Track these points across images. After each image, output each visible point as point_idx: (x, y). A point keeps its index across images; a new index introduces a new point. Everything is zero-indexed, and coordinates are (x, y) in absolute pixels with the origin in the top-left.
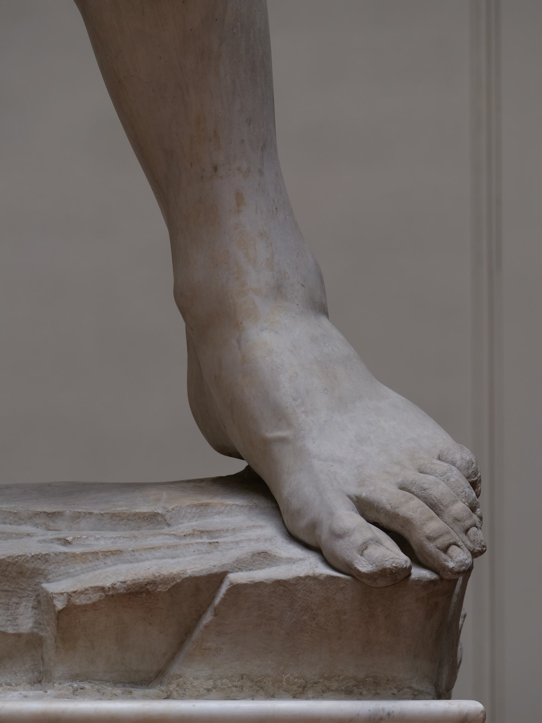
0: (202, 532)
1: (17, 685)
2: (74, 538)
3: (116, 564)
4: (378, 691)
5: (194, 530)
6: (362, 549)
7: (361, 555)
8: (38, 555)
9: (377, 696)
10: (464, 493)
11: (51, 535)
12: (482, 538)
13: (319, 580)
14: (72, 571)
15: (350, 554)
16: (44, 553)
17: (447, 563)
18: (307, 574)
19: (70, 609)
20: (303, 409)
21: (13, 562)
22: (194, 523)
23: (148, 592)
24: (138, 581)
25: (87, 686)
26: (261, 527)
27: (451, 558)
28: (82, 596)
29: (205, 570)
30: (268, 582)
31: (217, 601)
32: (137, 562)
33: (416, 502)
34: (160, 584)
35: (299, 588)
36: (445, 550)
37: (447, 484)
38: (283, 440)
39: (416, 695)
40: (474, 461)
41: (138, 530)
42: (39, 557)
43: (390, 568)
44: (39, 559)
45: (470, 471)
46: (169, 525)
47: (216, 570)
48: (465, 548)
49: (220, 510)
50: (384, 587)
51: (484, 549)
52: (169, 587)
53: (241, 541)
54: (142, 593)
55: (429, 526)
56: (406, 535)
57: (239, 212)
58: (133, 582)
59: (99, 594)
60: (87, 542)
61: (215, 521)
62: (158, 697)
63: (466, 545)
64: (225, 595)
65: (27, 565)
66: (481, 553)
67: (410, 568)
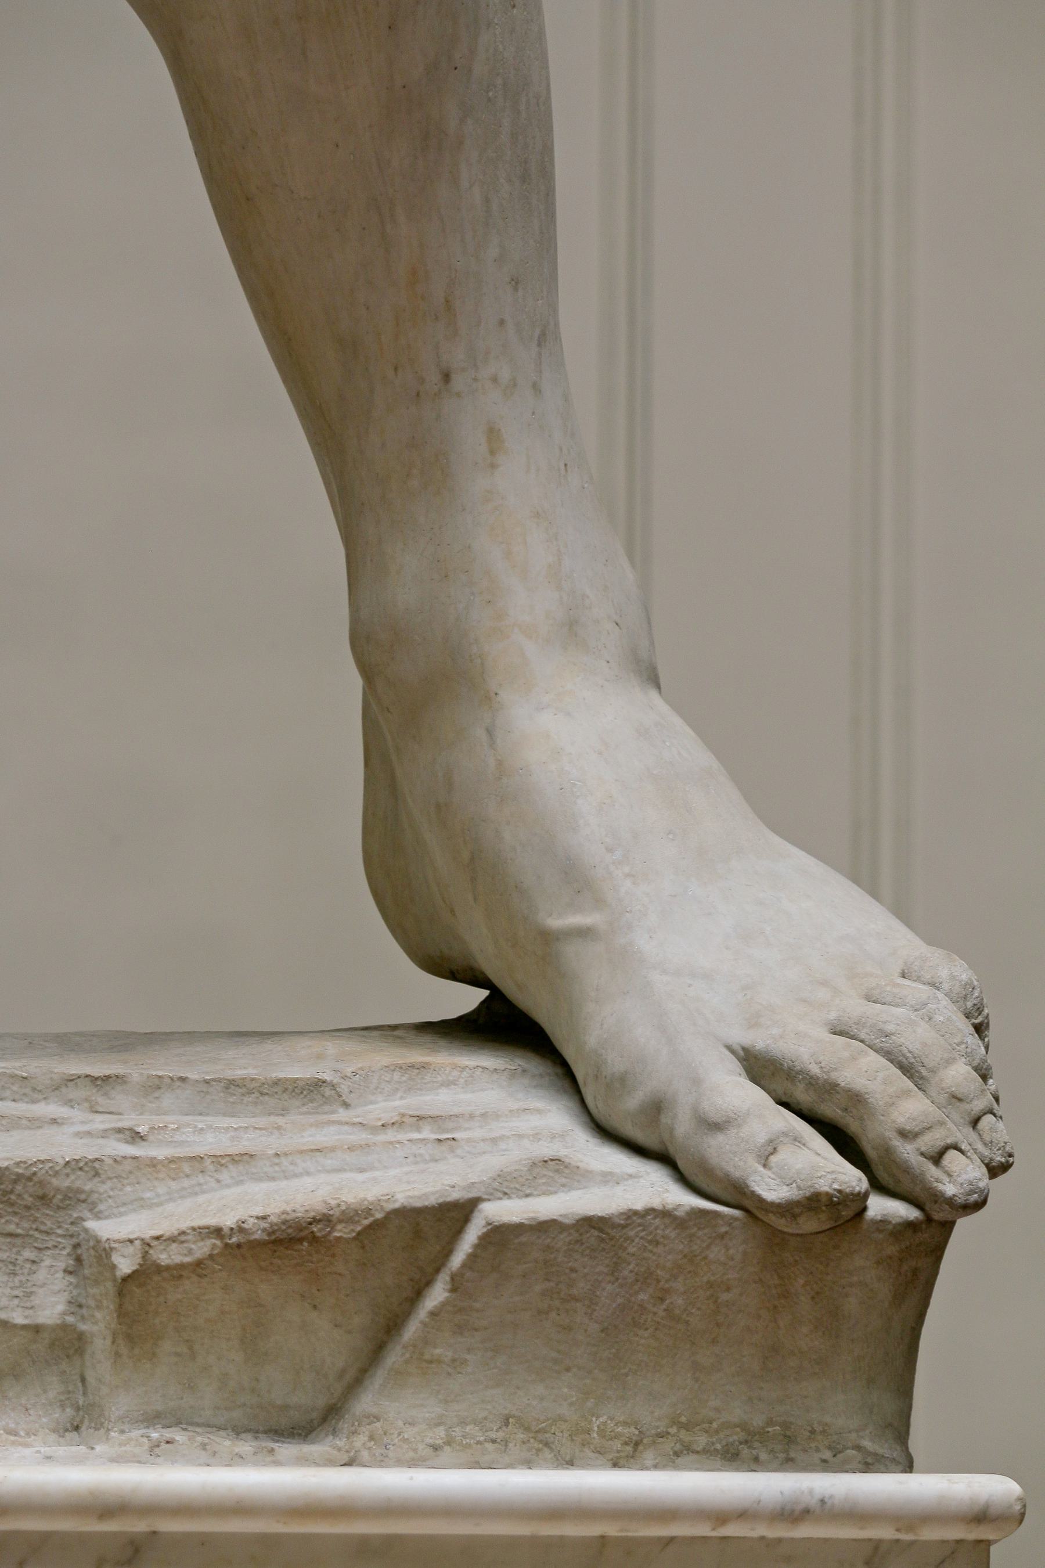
0: (421, 1118)
1: (28, 1434)
4: (792, 1455)
5: (403, 1115)
6: (767, 1153)
7: (765, 1166)
8: (77, 1161)
9: (788, 1464)
10: (963, 1046)
11: (101, 1122)
12: (1006, 1138)
14: (148, 1195)
15: (741, 1164)
16: (90, 1157)
17: (941, 1187)
18: (649, 1206)
19: (148, 1272)
20: (627, 869)
21: (28, 1173)
22: (398, 1103)
23: (314, 1239)
24: (294, 1215)
25: (179, 1436)
26: (539, 1111)
27: (949, 1175)
28: (174, 1246)
29: (433, 1193)
30: (566, 1221)
31: (457, 1259)
32: (286, 1178)
34: (340, 1221)
35: (632, 1233)
36: (937, 1158)
37: (930, 1024)
38: (584, 933)
39: (870, 1464)
40: (976, 983)
41: (282, 1115)
42: (81, 1165)
43: (827, 1194)
44: (81, 1169)
45: (969, 1004)
46: (346, 1105)
47: (455, 1195)
48: (975, 1157)
49: (451, 1078)
50: (811, 1234)
51: (1011, 1160)
52: (359, 1228)
53: (502, 1138)
55: (899, 1110)
56: (853, 1126)
57: (493, 466)
58: (283, 1217)
59: (210, 1242)
60: (178, 1137)
61: (440, 1100)
62: (330, 1462)
63: (975, 1150)
64: (476, 1247)
65: (55, 1182)
66: (1005, 1167)
67: (865, 1196)
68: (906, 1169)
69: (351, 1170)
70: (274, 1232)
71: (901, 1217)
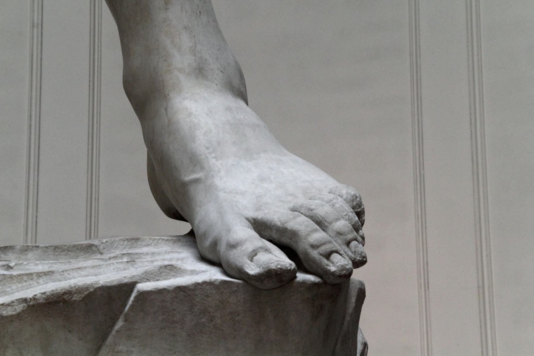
2: (16, 265)
3: (47, 283)
7: (251, 261)
13: (215, 285)
14: (8, 289)
15: (241, 260)
17: (329, 268)
20: (213, 155)
23: (65, 301)
24: (56, 292)
27: (333, 263)
28: (9, 308)
29: (116, 280)
32: (65, 280)
33: (303, 219)
34: (75, 293)
35: (197, 293)
36: (328, 256)
38: (197, 181)
43: (274, 269)
45: (355, 203)
46: (101, 254)
47: (126, 281)
48: (346, 257)
54: (59, 302)
56: (294, 246)
57: (167, 9)
59: (22, 305)
60: (26, 267)
63: (348, 255)
64: (133, 301)
68: (314, 261)
69: (92, 275)
70: (48, 299)
71: (312, 281)
